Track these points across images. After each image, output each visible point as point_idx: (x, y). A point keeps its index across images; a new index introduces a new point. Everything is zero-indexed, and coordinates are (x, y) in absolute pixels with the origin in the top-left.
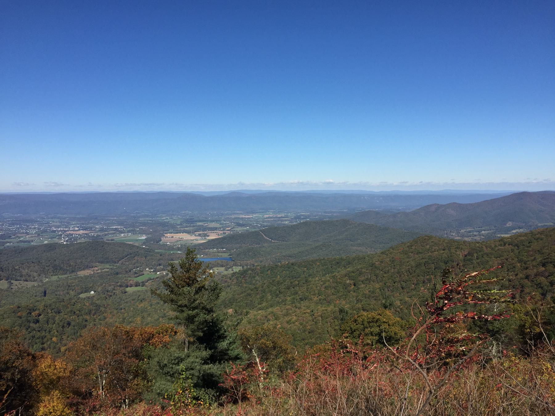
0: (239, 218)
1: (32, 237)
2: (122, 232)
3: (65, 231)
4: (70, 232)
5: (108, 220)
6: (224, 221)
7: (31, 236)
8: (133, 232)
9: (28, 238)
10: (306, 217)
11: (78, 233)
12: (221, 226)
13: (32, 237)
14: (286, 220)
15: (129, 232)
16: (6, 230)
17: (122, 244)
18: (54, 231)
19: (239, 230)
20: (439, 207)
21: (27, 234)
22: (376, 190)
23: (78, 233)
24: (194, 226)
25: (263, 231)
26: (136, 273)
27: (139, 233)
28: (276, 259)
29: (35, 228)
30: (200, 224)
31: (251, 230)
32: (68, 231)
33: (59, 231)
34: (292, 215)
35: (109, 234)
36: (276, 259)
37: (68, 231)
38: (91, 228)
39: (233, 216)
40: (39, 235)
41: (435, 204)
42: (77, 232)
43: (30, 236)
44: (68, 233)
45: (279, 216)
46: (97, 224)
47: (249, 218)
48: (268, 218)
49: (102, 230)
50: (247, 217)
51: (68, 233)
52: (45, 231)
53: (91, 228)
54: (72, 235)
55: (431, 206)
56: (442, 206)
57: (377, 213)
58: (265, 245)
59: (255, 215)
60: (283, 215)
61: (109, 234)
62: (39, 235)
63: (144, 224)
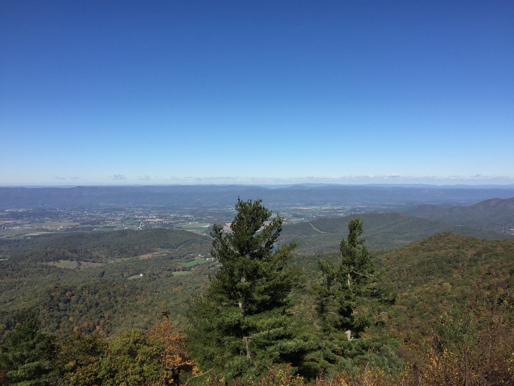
0: (297, 210)
1: (116, 223)
2: (191, 221)
3: (144, 219)
4: (148, 220)
5: (181, 210)
6: (283, 212)
7: (116, 223)
8: (200, 221)
9: (113, 224)
10: (362, 209)
11: (154, 220)
13: (116, 223)
14: (341, 213)
15: (196, 220)
16: (97, 218)
18: (136, 219)
19: (295, 221)
20: (500, 201)
21: (114, 220)
23: (154, 220)
25: (313, 222)
26: (188, 259)
28: (318, 249)
29: (121, 216)
31: (305, 221)
32: (147, 218)
33: (139, 219)
34: (348, 208)
35: (179, 222)
36: (318, 249)
37: (147, 218)
38: (166, 217)
39: (292, 208)
40: (122, 222)
41: (497, 199)
42: (154, 220)
43: (115, 222)
45: (336, 208)
46: (172, 213)
47: (307, 210)
48: (325, 210)
49: (175, 218)
50: (305, 208)
52: (128, 219)
53: (166, 217)
54: (149, 222)
55: (491, 200)
56: (503, 201)
57: (433, 207)
58: (314, 236)
59: (313, 207)
60: (340, 207)
61: (179, 222)
62: (122, 222)
63: (211, 214)
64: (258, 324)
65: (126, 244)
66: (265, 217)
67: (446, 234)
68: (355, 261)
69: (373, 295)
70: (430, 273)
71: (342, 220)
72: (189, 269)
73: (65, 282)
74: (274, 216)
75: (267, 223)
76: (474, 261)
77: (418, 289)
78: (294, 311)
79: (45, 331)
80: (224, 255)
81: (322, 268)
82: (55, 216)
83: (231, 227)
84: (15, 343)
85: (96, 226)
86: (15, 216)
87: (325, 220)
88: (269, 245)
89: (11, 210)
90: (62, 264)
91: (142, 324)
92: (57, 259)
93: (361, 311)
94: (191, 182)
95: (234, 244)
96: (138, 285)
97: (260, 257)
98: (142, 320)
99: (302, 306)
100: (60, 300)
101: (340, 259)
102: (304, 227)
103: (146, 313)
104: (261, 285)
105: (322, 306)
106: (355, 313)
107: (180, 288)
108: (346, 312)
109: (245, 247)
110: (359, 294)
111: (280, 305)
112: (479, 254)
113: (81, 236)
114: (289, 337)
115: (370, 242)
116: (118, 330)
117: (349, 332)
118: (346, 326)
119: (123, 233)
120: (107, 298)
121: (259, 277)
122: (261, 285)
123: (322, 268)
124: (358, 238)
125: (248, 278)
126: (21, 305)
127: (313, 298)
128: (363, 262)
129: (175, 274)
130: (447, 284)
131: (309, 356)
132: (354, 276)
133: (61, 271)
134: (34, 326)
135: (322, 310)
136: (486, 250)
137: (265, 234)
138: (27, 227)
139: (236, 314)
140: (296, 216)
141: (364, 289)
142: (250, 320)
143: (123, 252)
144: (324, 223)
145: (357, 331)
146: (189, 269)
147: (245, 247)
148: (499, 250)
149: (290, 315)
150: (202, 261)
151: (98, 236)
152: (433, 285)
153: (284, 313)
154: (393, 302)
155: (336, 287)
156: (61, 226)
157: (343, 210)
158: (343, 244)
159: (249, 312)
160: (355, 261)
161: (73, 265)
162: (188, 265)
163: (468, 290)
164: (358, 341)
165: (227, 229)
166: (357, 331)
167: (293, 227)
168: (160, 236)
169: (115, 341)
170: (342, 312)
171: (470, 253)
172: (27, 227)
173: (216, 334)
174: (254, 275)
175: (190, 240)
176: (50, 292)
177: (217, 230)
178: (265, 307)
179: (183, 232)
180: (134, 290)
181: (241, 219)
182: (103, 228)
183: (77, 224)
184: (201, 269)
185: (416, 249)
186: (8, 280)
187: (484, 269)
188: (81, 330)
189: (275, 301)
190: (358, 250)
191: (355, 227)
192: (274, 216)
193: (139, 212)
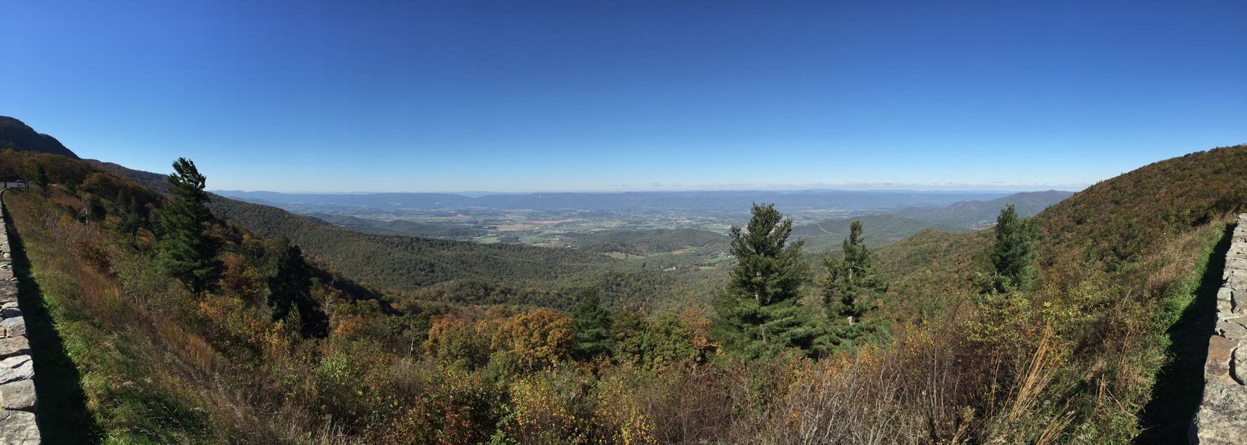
7: (654, 224)
19: (805, 222)
22: (923, 190)
34: (851, 211)
42: (685, 222)
64: (772, 314)
65: (663, 241)
66: (777, 220)
67: (928, 231)
68: (856, 257)
69: (871, 285)
70: (916, 263)
71: (845, 221)
72: (714, 265)
73: (617, 270)
74: (784, 218)
75: (778, 224)
76: (947, 251)
77: (906, 278)
78: (805, 301)
79: (603, 306)
80: (741, 253)
81: (827, 264)
82: (610, 216)
83: (750, 228)
84: (583, 312)
86: (584, 215)
87: (832, 221)
88: (781, 244)
90: (615, 255)
91: (675, 309)
92: (611, 251)
93: (862, 299)
94: (715, 189)
95: (750, 242)
96: (672, 276)
97: (773, 255)
98: (675, 306)
99: (810, 297)
100: (614, 282)
101: (844, 256)
102: (813, 228)
103: (679, 300)
104: (774, 279)
105: (828, 297)
106: (855, 301)
107: (706, 281)
108: (848, 301)
109: (762, 246)
110: (859, 285)
111: (790, 296)
112: (951, 246)
113: (628, 233)
114: (799, 324)
115: (869, 240)
116: (657, 312)
117: (850, 318)
118: (848, 313)
119: (660, 232)
120: (649, 285)
121: (772, 272)
122: (774, 279)
123: (827, 264)
124: (858, 238)
125: (763, 274)
126: (587, 284)
127: (820, 290)
128: (862, 259)
129: (702, 268)
130: (928, 271)
131: (816, 341)
132: (855, 270)
133: (615, 261)
134: (596, 301)
135: (828, 300)
136: (956, 242)
137: (777, 235)
138: (591, 224)
139: (752, 305)
140: (806, 218)
141: (863, 281)
142: (764, 308)
143: (659, 248)
144: (829, 224)
145: (857, 316)
146: (714, 265)
147: (762, 246)
148: (965, 241)
149: (799, 305)
150: (725, 258)
151: (641, 234)
152: (918, 274)
153: (794, 303)
154: (885, 290)
155: (839, 280)
156: (614, 224)
157: (847, 213)
158: (845, 243)
159: (763, 303)
160: (856, 257)
161: (622, 256)
162: (713, 261)
163: (943, 275)
164: (858, 324)
165: (745, 231)
166: (857, 316)
167: (802, 229)
168: (690, 235)
169: (654, 320)
170: (844, 301)
171: (945, 245)
172: (591, 224)
173: (736, 321)
174: (767, 271)
175: (714, 239)
176: (606, 276)
177: (735, 231)
178: (778, 298)
179: (709, 232)
180: (669, 280)
181: (757, 221)
184: (722, 265)
185: (905, 245)
186: (578, 264)
187: (954, 256)
188: (628, 309)
189: (787, 292)
190: (858, 248)
191: (855, 228)
192: (784, 218)
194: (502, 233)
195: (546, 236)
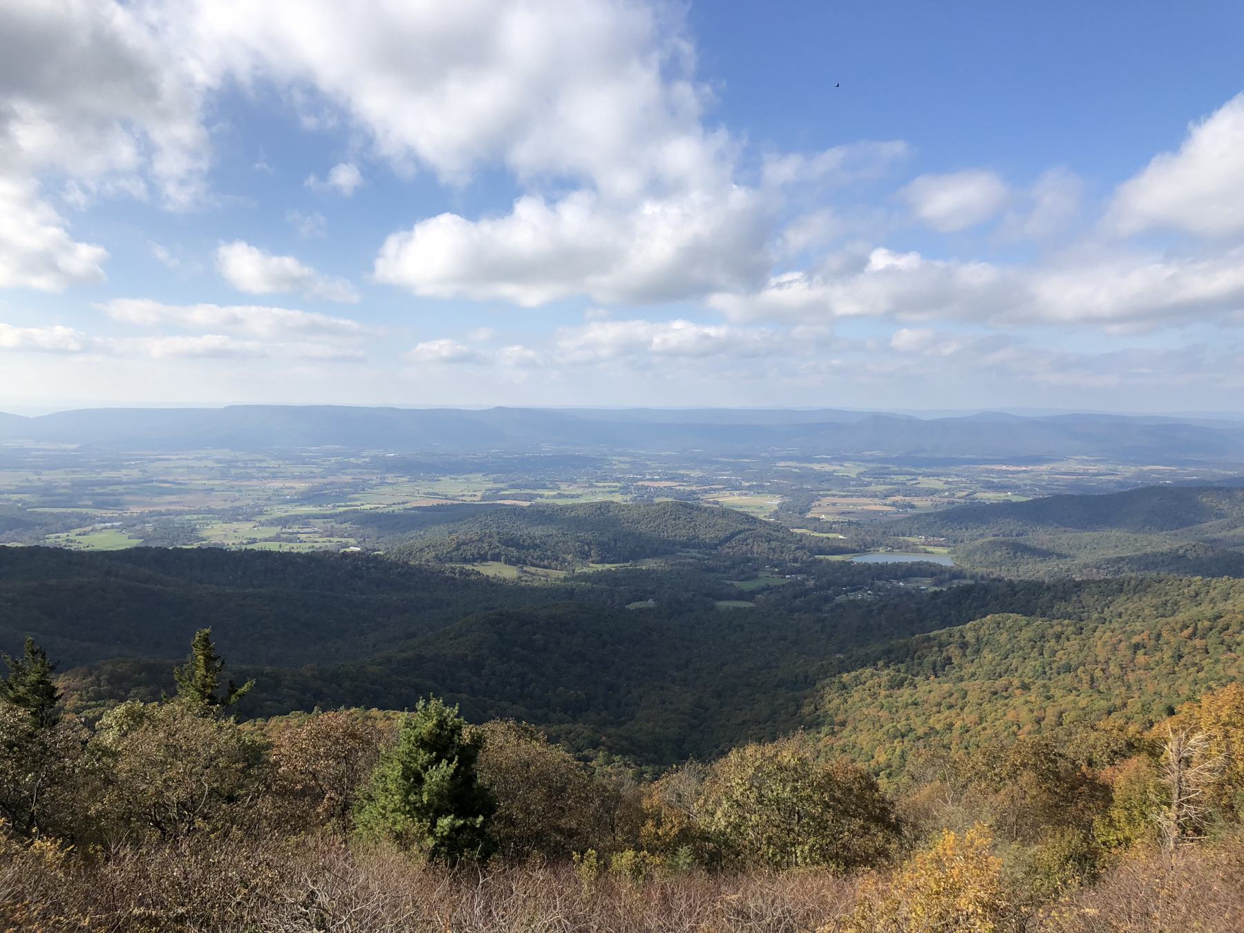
0: (992, 471)
4: (646, 484)
11: (656, 484)
12: (946, 487)
17: (725, 513)
19: (991, 497)
23: (656, 484)
24: (885, 484)
27: (771, 492)
30: (902, 478)
31: (1015, 499)
32: (641, 480)
44: (640, 483)
49: (700, 481)
51: (640, 483)
54: (646, 488)
63: (785, 475)
85: (540, 492)
89: (374, 452)
140: (990, 486)
182: (554, 497)
183: (502, 486)
193: (623, 466)
194: (142, 519)
195: (283, 522)
